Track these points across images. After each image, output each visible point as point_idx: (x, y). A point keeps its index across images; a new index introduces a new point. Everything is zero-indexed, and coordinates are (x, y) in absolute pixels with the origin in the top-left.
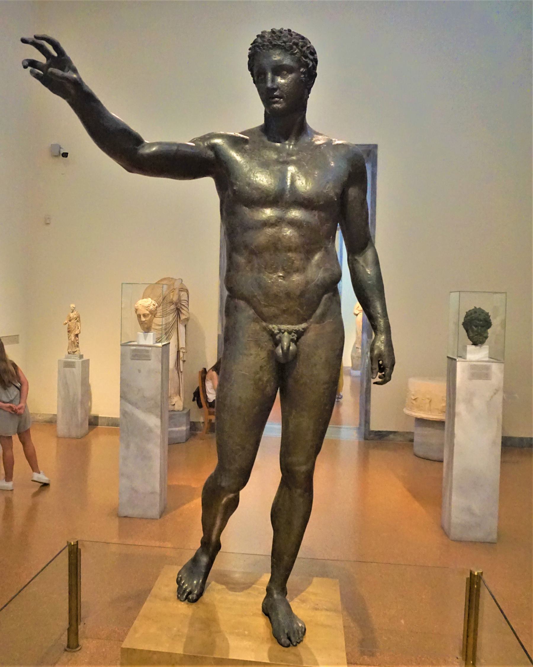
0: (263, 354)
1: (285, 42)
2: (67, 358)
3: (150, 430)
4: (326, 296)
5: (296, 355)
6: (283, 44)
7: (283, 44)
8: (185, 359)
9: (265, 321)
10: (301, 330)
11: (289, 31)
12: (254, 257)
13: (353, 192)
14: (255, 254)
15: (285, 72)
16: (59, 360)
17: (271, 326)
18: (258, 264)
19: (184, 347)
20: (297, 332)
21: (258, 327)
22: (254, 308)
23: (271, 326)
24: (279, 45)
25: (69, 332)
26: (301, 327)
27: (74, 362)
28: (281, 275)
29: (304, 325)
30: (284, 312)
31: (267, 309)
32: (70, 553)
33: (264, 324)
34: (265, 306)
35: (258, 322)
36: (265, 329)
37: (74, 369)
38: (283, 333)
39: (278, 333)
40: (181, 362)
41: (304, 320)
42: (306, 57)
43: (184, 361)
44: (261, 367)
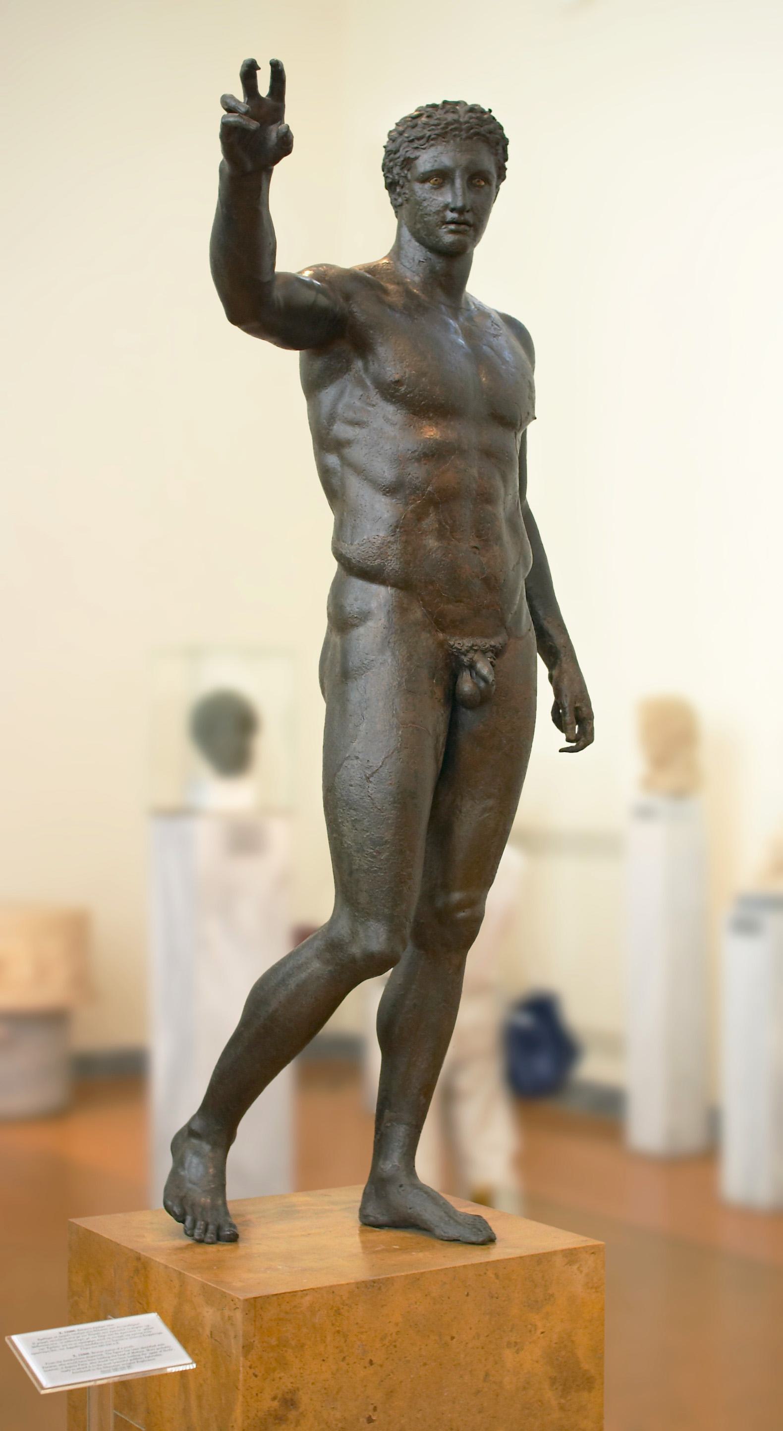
0: (439, 693)
1: (490, 132)
6: (488, 135)
7: (488, 135)
9: (443, 631)
10: (498, 645)
12: (431, 509)
14: (436, 505)
15: (483, 183)
18: (440, 523)
21: (431, 641)
24: (484, 136)
28: (473, 544)
31: (451, 606)
33: (441, 636)
35: (430, 632)
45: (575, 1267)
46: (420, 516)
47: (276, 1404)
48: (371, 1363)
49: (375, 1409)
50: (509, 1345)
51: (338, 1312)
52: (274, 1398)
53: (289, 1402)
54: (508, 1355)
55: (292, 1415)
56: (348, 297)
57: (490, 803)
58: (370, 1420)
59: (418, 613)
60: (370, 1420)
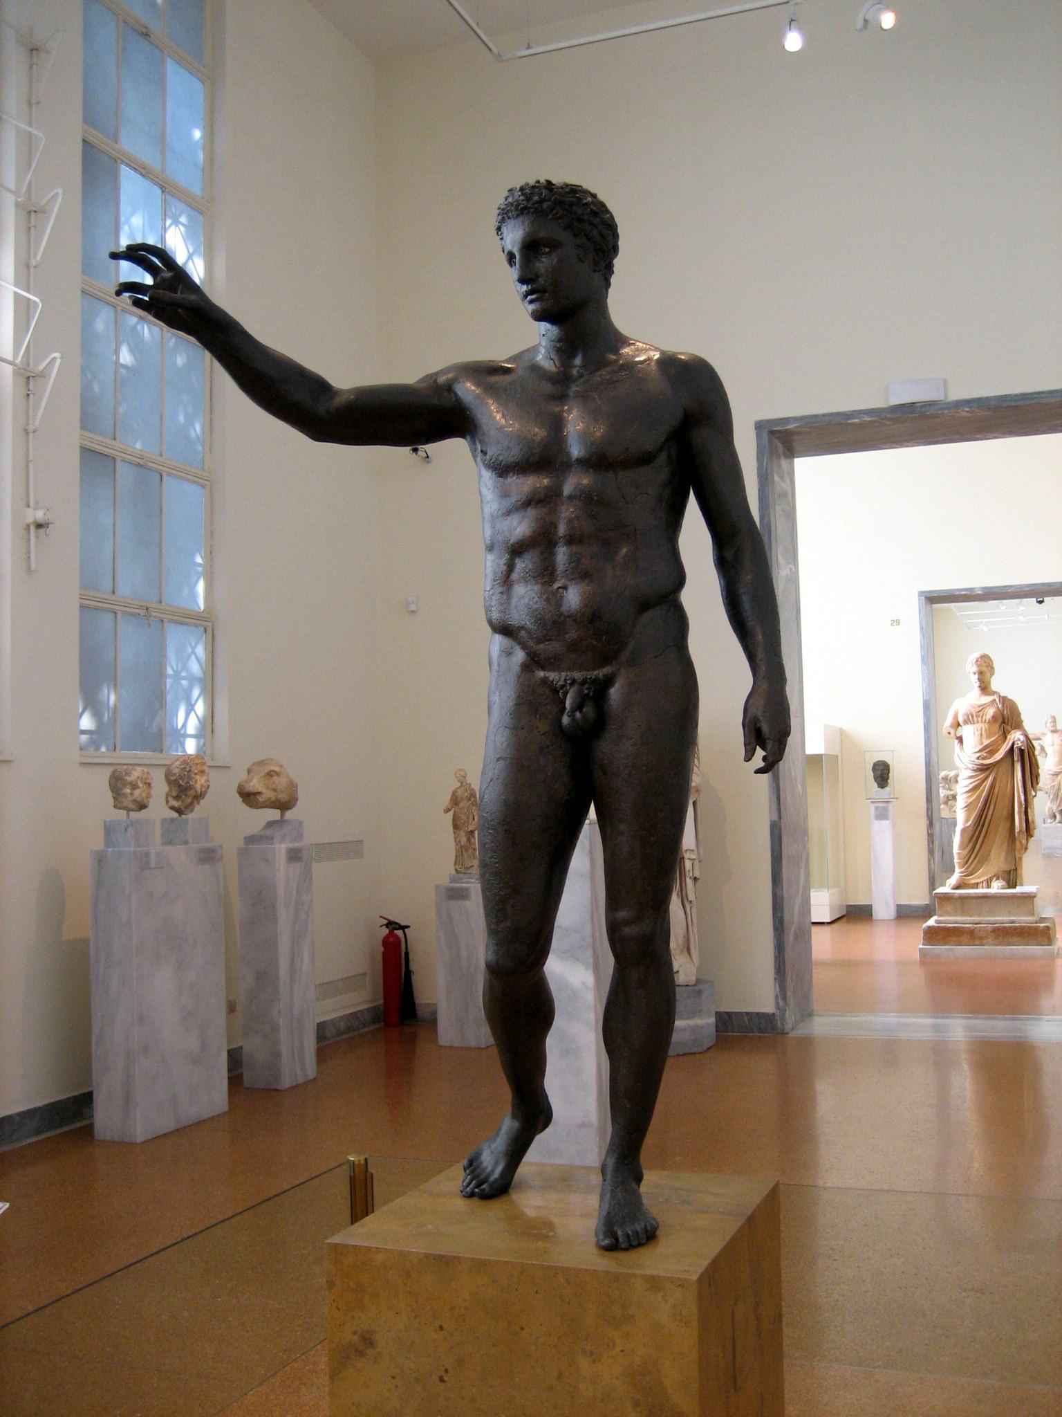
0: (543, 726)
2: (453, 880)
3: (574, 996)
4: (647, 616)
5: (598, 725)
8: (697, 874)
11: (549, 182)
13: (702, 436)
16: (437, 887)
17: (552, 676)
19: (693, 847)
20: (595, 681)
22: (524, 646)
23: (552, 676)
25: (456, 827)
26: (601, 673)
27: (467, 890)
29: (606, 670)
30: (574, 647)
31: (541, 646)
32: (352, 1180)
33: (542, 674)
34: (539, 641)
36: (545, 681)
37: (467, 903)
38: (572, 684)
39: (563, 687)
40: (689, 882)
41: (605, 660)
42: (580, 220)
43: (695, 879)
44: (541, 749)
45: (660, 1295)
46: (510, 567)
47: (356, 1338)
48: (441, 1328)
49: (446, 1371)
50: (584, 1352)
51: (408, 1274)
52: (354, 1333)
53: (368, 1340)
54: (583, 1362)
55: (370, 1352)
56: (449, 388)
57: (622, 827)
58: (442, 1380)
59: (520, 656)
60: (442, 1380)
